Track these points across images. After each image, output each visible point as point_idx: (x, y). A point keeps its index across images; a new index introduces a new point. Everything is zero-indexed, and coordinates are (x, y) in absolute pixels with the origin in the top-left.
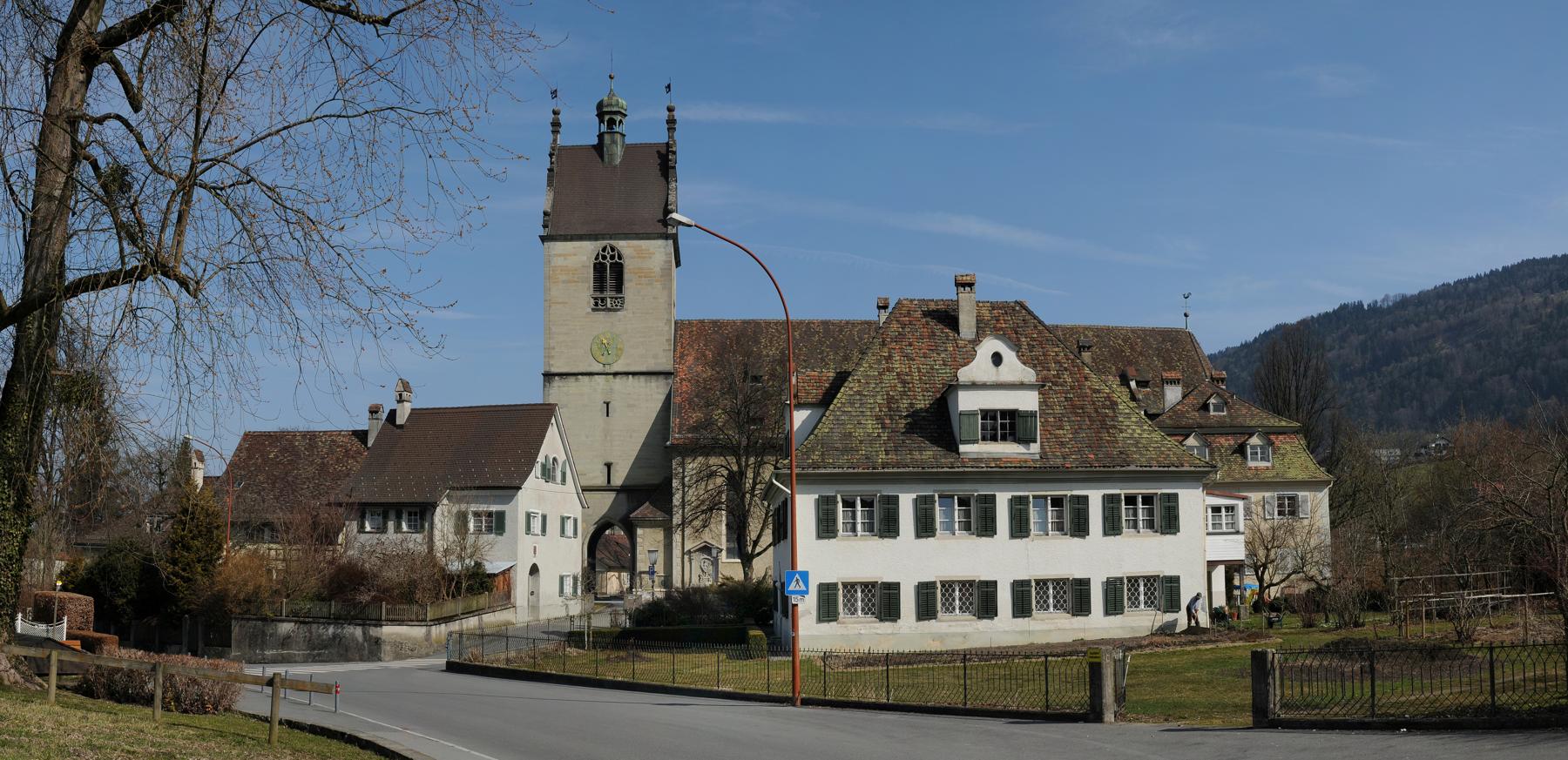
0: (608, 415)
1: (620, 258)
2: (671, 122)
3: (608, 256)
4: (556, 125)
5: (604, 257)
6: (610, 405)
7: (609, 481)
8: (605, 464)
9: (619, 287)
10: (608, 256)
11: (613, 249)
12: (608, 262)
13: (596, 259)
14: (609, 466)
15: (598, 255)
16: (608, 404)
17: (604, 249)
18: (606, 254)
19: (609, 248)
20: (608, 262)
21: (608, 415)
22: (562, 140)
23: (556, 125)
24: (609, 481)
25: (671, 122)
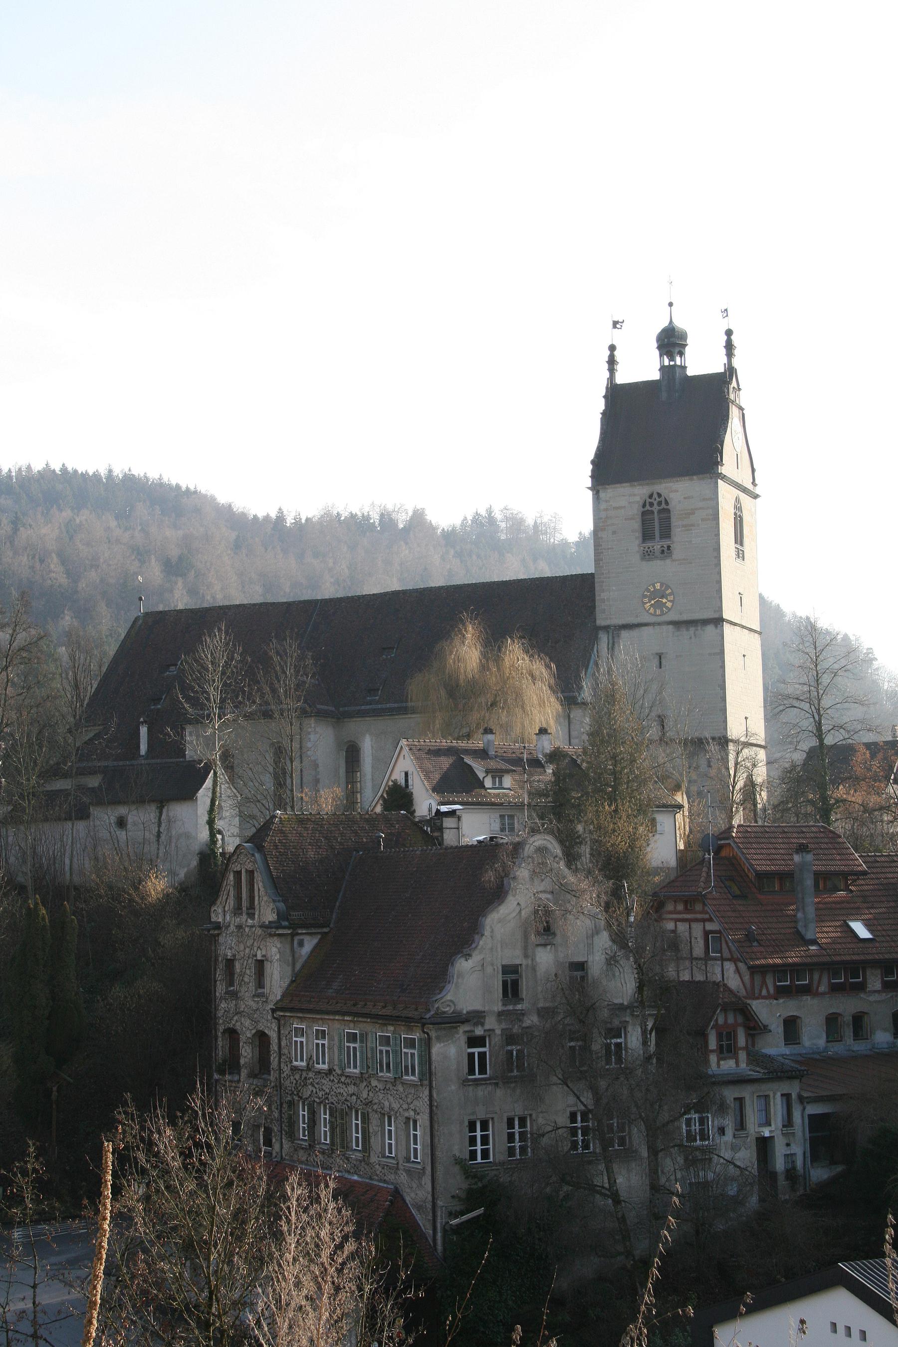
1: (667, 503)
2: (729, 347)
3: (655, 503)
4: (612, 362)
9: (666, 533)
10: (655, 503)
11: (659, 495)
12: (656, 508)
13: (644, 506)
17: (651, 496)
19: (655, 496)
20: (656, 508)
22: (621, 379)
23: (612, 362)
25: (729, 347)
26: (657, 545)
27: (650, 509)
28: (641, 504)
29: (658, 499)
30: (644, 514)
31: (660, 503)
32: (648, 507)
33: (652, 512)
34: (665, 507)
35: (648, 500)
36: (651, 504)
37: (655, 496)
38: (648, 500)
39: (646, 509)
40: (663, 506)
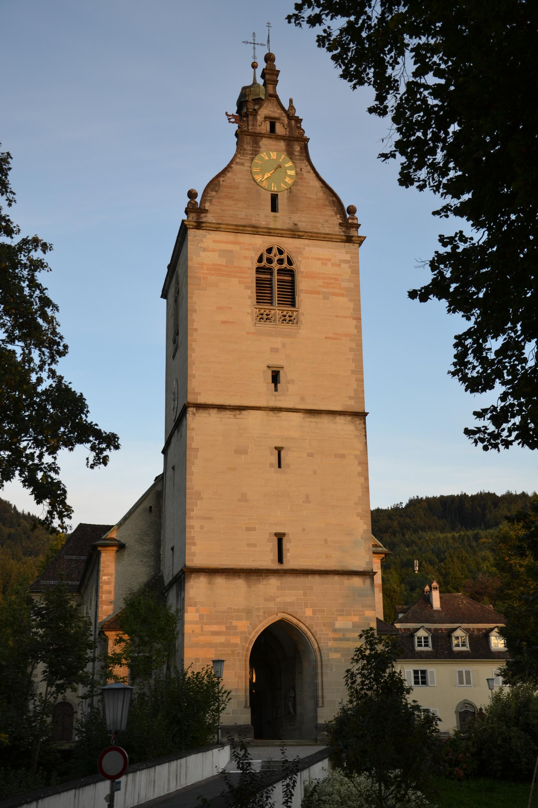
0: (280, 466)
1: (290, 263)
5: (270, 261)
6: (282, 453)
7: (280, 560)
8: (276, 534)
10: (275, 262)
11: (281, 252)
12: (275, 266)
13: (260, 260)
14: (280, 538)
15: (261, 256)
16: (279, 450)
17: (269, 250)
19: (275, 251)
21: (280, 466)
24: (280, 560)
26: (277, 311)
29: (279, 257)
30: (259, 270)
31: (280, 261)
34: (289, 267)
36: (270, 261)
37: (275, 251)
39: (262, 264)
40: (285, 265)
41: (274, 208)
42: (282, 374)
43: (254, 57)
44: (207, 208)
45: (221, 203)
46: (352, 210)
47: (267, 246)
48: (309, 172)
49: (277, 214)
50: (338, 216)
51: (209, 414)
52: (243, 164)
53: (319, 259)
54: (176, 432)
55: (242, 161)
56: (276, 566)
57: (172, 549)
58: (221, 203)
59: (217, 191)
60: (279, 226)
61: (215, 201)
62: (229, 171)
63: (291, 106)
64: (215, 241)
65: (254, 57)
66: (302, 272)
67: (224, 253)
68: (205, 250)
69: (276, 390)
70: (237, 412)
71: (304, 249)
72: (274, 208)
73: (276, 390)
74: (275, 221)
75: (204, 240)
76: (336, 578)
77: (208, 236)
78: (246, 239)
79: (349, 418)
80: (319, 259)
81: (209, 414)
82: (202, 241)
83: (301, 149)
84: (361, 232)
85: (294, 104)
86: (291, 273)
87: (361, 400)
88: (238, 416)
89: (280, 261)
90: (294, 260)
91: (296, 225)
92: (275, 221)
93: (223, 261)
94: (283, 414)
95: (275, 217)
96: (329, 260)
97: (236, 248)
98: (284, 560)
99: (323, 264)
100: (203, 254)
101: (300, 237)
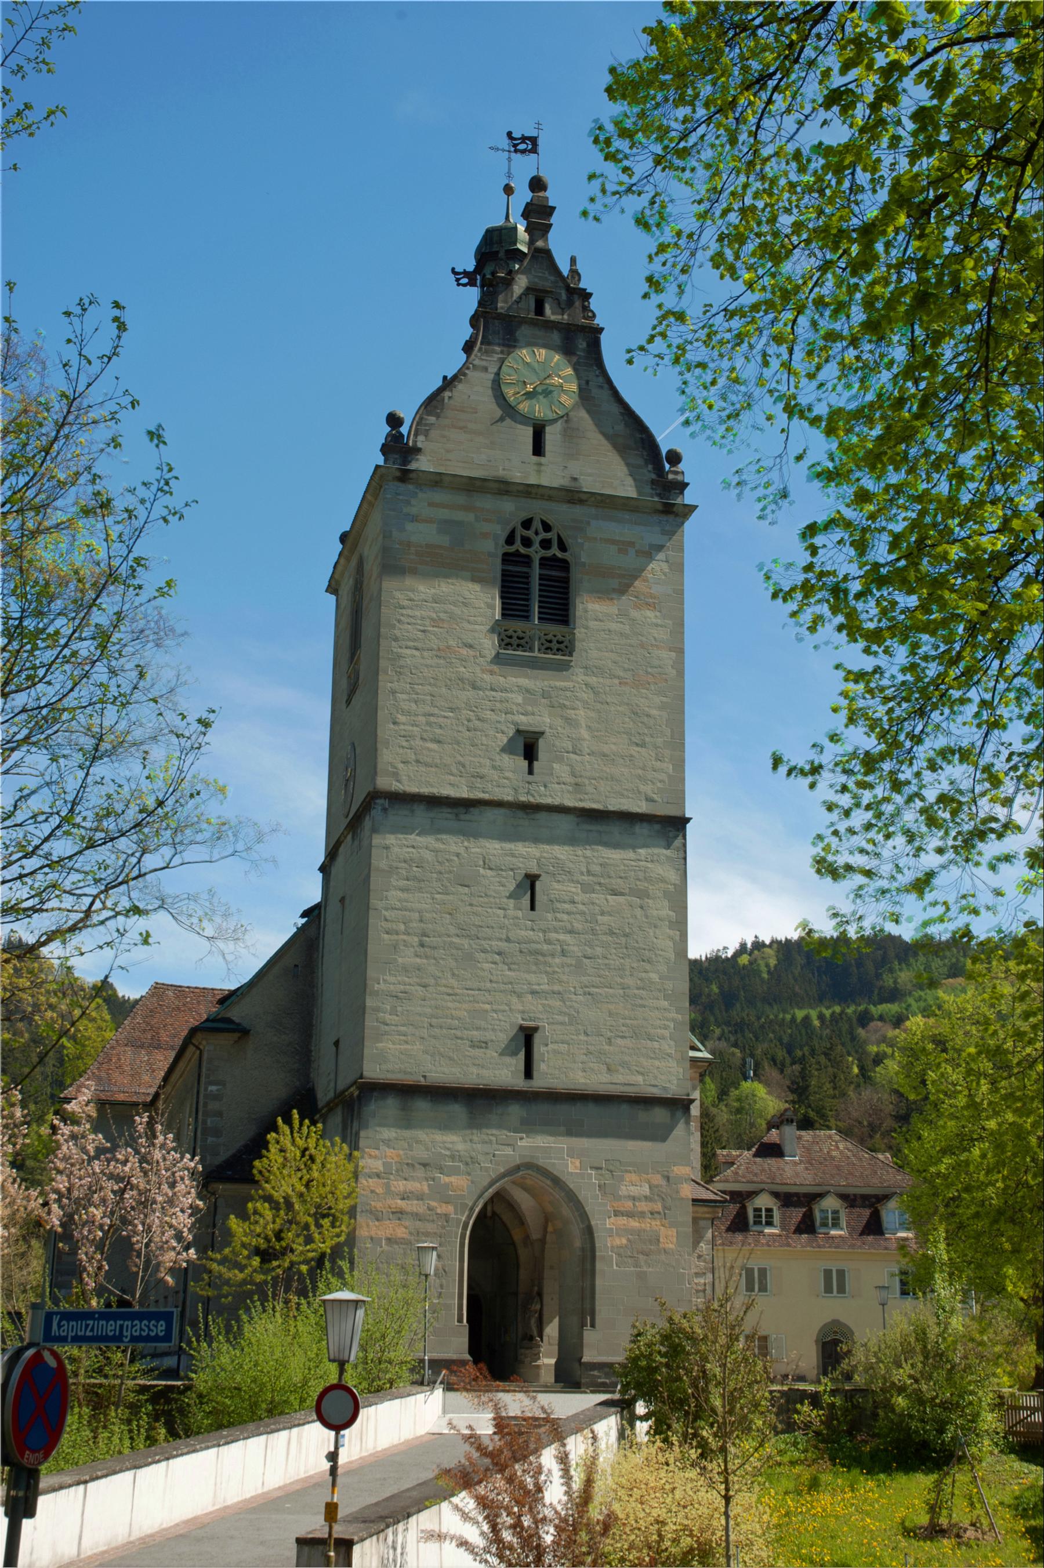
0: (533, 908)
1: (563, 547)
5: (527, 542)
7: (528, 1073)
10: (536, 545)
11: (547, 527)
12: (536, 553)
13: (510, 540)
17: (527, 524)
18: (530, 533)
20: (536, 553)
24: (528, 1073)
27: (523, 550)
28: (504, 535)
29: (543, 535)
30: (507, 558)
31: (546, 544)
32: (518, 546)
33: (527, 560)
35: (520, 532)
36: (527, 542)
37: (537, 524)
38: (520, 532)
40: (555, 551)
41: (538, 449)
42: (543, 747)
43: (509, 175)
44: (419, 445)
45: (444, 437)
46: (674, 458)
47: (524, 515)
48: (601, 387)
49: (542, 460)
50: (650, 467)
51: (412, 811)
52: (485, 369)
53: (613, 542)
54: (349, 837)
55: (484, 363)
56: (519, 1082)
57: (337, 1044)
58: (444, 437)
59: (438, 416)
60: (545, 481)
61: (433, 433)
62: (460, 381)
63: (575, 273)
64: (431, 504)
65: (509, 175)
66: (584, 564)
67: (446, 526)
68: (414, 519)
69: (531, 772)
70: (462, 810)
71: (588, 523)
72: (538, 449)
73: (531, 772)
74: (539, 472)
75: (413, 502)
76: (625, 1107)
77: (421, 495)
78: (486, 502)
79: (657, 827)
80: (613, 542)
81: (412, 811)
82: (408, 503)
83: (588, 345)
84: (689, 497)
85: (579, 267)
86: (564, 565)
87: (680, 798)
88: (462, 817)
89: (546, 544)
90: (569, 542)
91: (575, 479)
92: (539, 472)
93: (444, 540)
94: (542, 816)
95: (540, 464)
96: (632, 544)
97: (470, 517)
98: (535, 1074)
99: (620, 551)
100: (410, 527)
101: (581, 502)
